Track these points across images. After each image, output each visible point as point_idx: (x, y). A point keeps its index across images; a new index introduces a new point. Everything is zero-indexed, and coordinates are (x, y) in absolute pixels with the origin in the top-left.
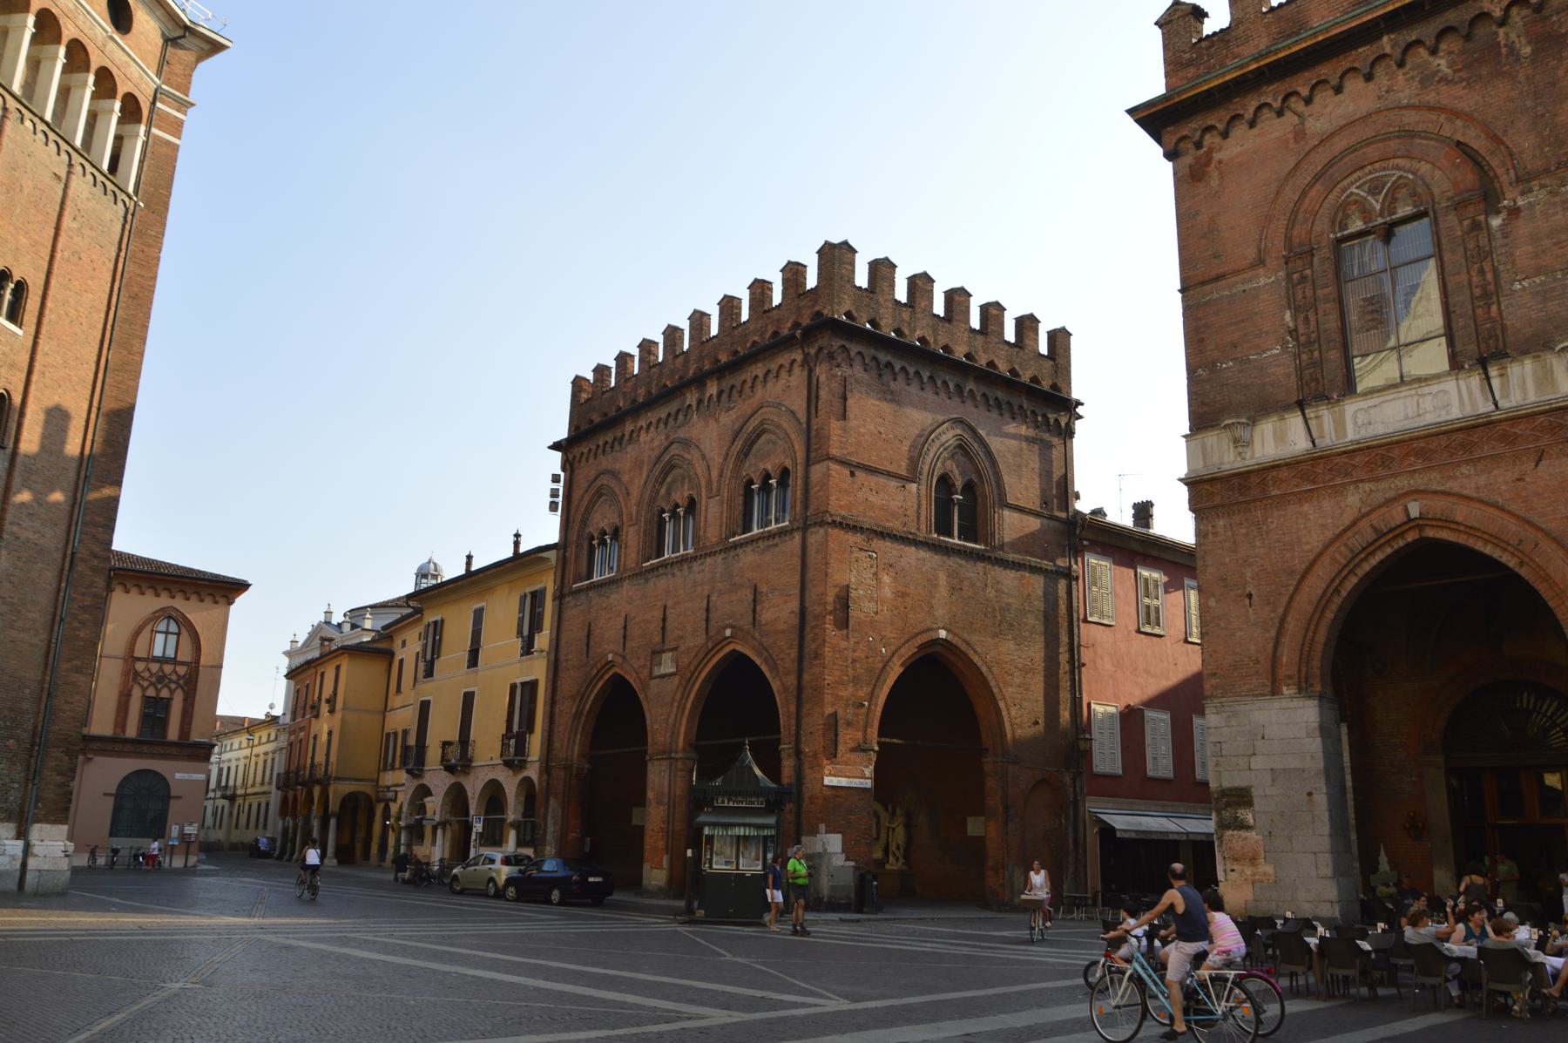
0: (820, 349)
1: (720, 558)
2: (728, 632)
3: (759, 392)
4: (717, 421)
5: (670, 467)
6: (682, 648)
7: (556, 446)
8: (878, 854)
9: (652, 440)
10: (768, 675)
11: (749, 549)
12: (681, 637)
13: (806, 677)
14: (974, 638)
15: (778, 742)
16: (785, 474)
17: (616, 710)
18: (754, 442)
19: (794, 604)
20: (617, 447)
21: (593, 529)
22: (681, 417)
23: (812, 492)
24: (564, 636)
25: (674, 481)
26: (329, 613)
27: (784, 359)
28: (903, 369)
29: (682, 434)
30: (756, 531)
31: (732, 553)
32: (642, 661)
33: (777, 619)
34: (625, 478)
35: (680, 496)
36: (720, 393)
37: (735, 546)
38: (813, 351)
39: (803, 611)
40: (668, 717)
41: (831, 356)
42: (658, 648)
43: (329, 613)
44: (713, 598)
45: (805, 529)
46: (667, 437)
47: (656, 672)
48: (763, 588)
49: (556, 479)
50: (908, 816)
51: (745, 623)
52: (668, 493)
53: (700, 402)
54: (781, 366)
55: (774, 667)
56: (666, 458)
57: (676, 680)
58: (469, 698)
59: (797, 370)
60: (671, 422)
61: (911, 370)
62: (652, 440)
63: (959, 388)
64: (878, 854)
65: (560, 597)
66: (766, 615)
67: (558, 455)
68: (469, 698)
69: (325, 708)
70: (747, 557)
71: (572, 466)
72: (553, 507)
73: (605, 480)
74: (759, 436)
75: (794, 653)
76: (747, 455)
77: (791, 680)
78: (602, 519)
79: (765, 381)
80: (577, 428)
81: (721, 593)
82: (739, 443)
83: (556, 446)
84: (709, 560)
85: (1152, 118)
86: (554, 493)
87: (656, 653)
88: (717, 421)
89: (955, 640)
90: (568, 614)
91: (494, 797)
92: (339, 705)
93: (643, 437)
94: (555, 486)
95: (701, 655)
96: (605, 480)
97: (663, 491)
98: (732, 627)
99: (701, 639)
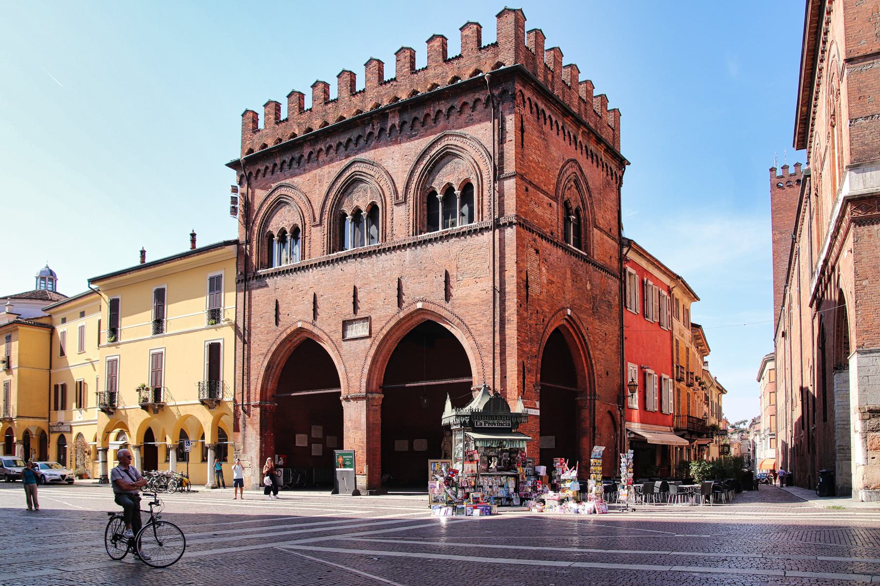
0: (505, 92)
7: (234, 165)
12: (371, 309)
14: (582, 316)
16: (467, 187)
17: (302, 364)
19: (487, 284)
20: (295, 165)
21: (274, 227)
22: (362, 141)
27: (469, 99)
28: (550, 116)
30: (441, 230)
33: (468, 295)
35: (360, 200)
36: (403, 123)
38: (496, 93)
41: (514, 97)
44: (403, 281)
48: (453, 273)
49: (235, 190)
53: (382, 130)
54: (465, 104)
56: (348, 173)
59: (480, 107)
60: (352, 146)
61: (554, 119)
67: (234, 172)
71: (248, 179)
72: (234, 211)
78: (282, 220)
79: (448, 116)
83: (234, 165)
86: (234, 201)
89: (574, 317)
92: (14, 364)
94: (234, 195)
96: (283, 191)
98: (423, 301)
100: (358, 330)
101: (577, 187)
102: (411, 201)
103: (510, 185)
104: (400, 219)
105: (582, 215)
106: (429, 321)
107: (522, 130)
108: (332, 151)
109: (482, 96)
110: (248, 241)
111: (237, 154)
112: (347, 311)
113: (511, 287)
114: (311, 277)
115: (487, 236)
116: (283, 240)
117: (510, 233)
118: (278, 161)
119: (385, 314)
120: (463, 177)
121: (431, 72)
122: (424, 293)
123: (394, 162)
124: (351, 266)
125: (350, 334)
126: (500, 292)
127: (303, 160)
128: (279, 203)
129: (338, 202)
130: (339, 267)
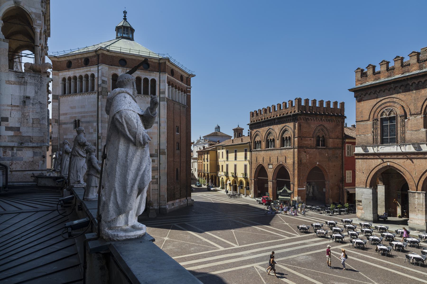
5: (270, 133)
7: (248, 124)
8: (308, 193)
19: (292, 161)
26: (200, 137)
40: (270, 171)
43: (200, 137)
48: (287, 157)
50: (313, 187)
55: (289, 170)
58: (235, 166)
61: (312, 118)
63: (321, 119)
64: (308, 193)
66: (288, 161)
68: (235, 166)
69: (206, 160)
80: (252, 122)
83: (248, 124)
85: (345, 117)
91: (241, 182)
96: (257, 132)
101: (323, 131)
102: (280, 139)
103: (296, 139)
104: (278, 143)
105: (325, 137)
107: (300, 126)
110: (251, 143)
111: (249, 123)
113: (296, 162)
115: (292, 150)
116: (258, 143)
117: (296, 150)
119: (275, 164)
120: (289, 135)
121: (283, 110)
122: (282, 160)
123: (277, 129)
124: (269, 152)
125: (269, 167)
126: (294, 163)
128: (257, 135)
129: (267, 137)
130: (267, 152)
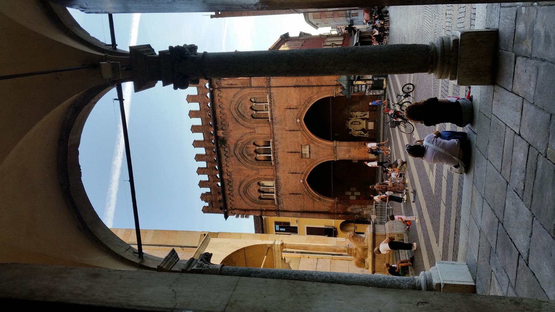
1: (275, 126)
2: (298, 121)
3: (225, 111)
4: (231, 131)
6: (301, 143)
7: (226, 217)
9: (232, 164)
10: (312, 103)
11: (273, 113)
13: (314, 84)
15: (332, 97)
18: (240, 114)
23: (260, 85)
24: (293, 209)
25: (247, 153)
29: (232, 148)
31: (274, 121)
32: (304, 163)
34: (243, 178)
37: (272, 119)
39: (295, 86)
42: (300, 155)
44: (287, 128)
45: (270, 87)
46: (232, 156)
47: (308, 156)
51: (296, 112)
52: (250, 155)
57: (312, 145)
59: (221, 94)
62: (232, 164)
65: (278, 212)
66: (294, 103)
70: (276, 114)
71: (233, 210)
73: (241, 190)
74: (239, 111)
75: (307, 89)
76: (244, 117)
77: (315, 90)
80: (221, 209)
81: (286, 125)
82: (240, 120)
83: (226, 217)
84: (275, 132)
87: (302, 156)
88: (231, 131)
90: (285, 208)
93: (230, 170)
95: (305, 134)
97: (249, 158)
99: (299, 133)
100: (306, 150)
106: (304, 120)
108: (228, 164)
109: (217, 92)
111: (222, 216)
112: (298, 156)
114: (281, 175)
118: (228, 192)
127: (229, 180)
